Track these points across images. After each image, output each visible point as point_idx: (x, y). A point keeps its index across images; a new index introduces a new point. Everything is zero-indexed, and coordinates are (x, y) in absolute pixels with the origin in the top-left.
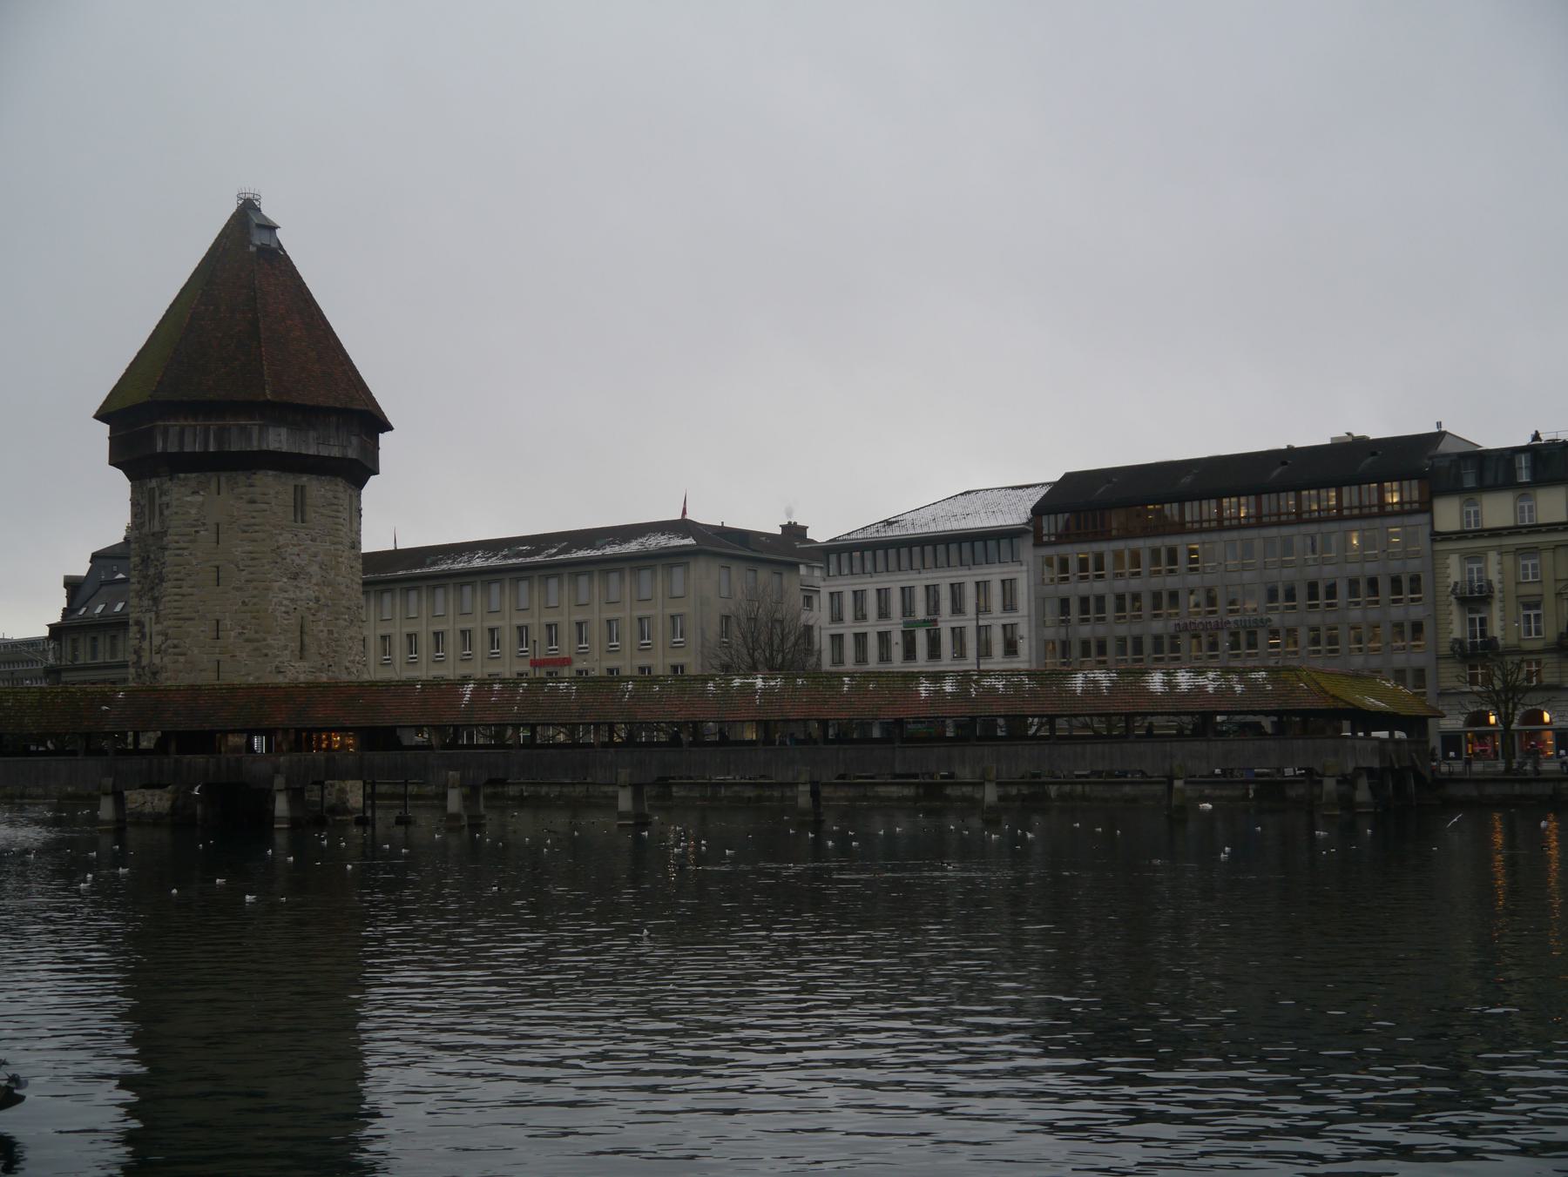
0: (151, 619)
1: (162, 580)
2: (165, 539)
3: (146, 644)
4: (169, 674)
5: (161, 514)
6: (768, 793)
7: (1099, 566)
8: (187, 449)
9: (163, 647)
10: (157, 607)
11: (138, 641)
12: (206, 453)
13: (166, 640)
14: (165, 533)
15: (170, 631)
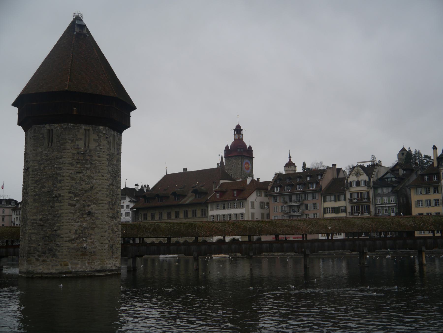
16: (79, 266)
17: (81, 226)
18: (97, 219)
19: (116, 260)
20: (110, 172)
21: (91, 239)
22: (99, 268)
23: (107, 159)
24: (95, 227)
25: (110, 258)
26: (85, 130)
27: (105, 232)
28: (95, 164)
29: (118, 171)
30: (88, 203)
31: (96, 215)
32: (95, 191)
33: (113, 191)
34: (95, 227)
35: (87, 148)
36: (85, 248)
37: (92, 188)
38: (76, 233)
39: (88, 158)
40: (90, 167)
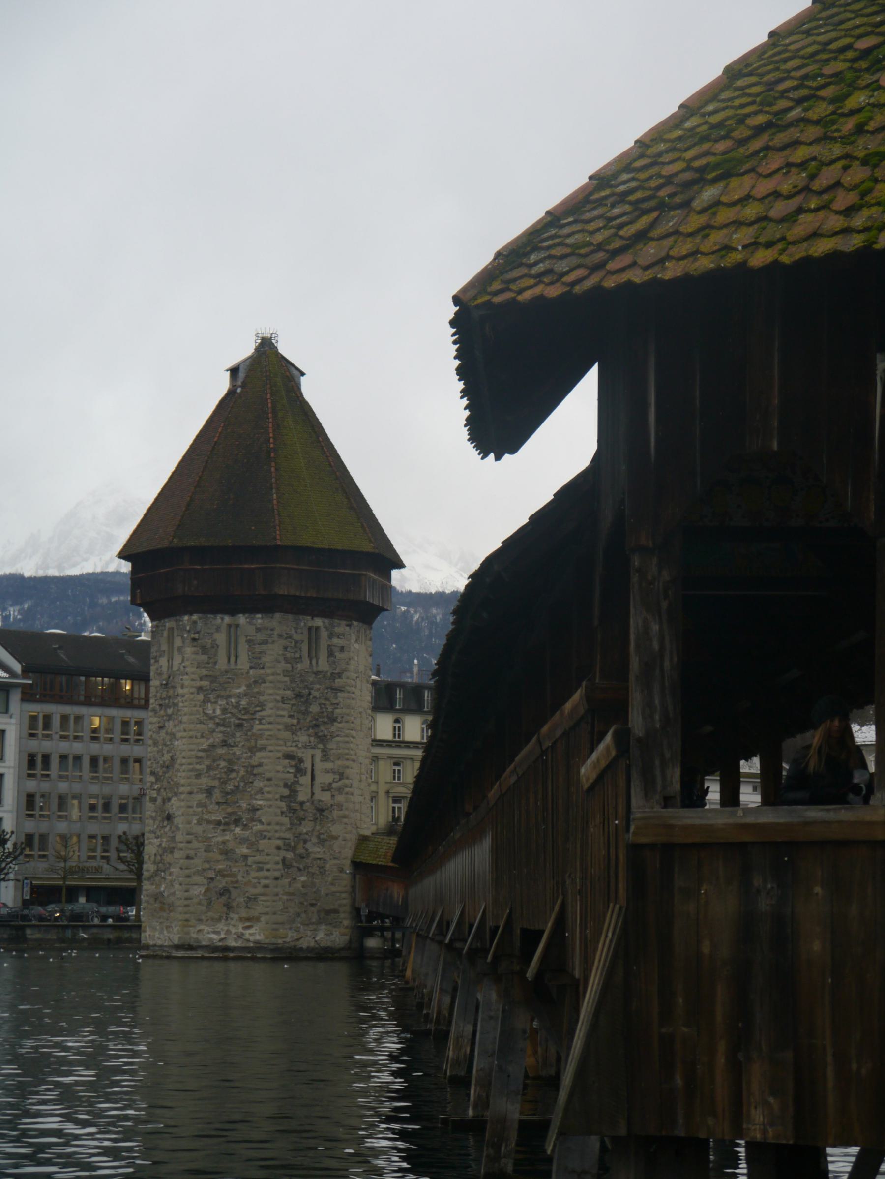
0: (313, 756)
1: (333, 720)
2: (337, 681)
3: (305, 780)
4: (347, 813)
5: (331, 654)
6: (126, 935)
7: (47, 725)
8: (375, 603)
9: (334, 785)
10: (325, 746)
11: (292, 775)
12: (379, 606)
13: (340, 780)
14: (340, 675)
15: (347, 771)
17: (160, 846)
18: (178, 828)
19: (247, 924)
20: (211, 718)
21: (171, 874)
22: (176, 942)
23: (200, 689)
24: (174, 848)
25: (219, 920)
26: (169, 628)
27: (188, 858)
29: (258, 709)
30: (170, 795)
31: (176, 821)
32: (177, 766)
33: (230, 762)
34: (174, 848)
35: (170, 670)
36: (161, 894)
37: (172, 759)
40: (173, 714)
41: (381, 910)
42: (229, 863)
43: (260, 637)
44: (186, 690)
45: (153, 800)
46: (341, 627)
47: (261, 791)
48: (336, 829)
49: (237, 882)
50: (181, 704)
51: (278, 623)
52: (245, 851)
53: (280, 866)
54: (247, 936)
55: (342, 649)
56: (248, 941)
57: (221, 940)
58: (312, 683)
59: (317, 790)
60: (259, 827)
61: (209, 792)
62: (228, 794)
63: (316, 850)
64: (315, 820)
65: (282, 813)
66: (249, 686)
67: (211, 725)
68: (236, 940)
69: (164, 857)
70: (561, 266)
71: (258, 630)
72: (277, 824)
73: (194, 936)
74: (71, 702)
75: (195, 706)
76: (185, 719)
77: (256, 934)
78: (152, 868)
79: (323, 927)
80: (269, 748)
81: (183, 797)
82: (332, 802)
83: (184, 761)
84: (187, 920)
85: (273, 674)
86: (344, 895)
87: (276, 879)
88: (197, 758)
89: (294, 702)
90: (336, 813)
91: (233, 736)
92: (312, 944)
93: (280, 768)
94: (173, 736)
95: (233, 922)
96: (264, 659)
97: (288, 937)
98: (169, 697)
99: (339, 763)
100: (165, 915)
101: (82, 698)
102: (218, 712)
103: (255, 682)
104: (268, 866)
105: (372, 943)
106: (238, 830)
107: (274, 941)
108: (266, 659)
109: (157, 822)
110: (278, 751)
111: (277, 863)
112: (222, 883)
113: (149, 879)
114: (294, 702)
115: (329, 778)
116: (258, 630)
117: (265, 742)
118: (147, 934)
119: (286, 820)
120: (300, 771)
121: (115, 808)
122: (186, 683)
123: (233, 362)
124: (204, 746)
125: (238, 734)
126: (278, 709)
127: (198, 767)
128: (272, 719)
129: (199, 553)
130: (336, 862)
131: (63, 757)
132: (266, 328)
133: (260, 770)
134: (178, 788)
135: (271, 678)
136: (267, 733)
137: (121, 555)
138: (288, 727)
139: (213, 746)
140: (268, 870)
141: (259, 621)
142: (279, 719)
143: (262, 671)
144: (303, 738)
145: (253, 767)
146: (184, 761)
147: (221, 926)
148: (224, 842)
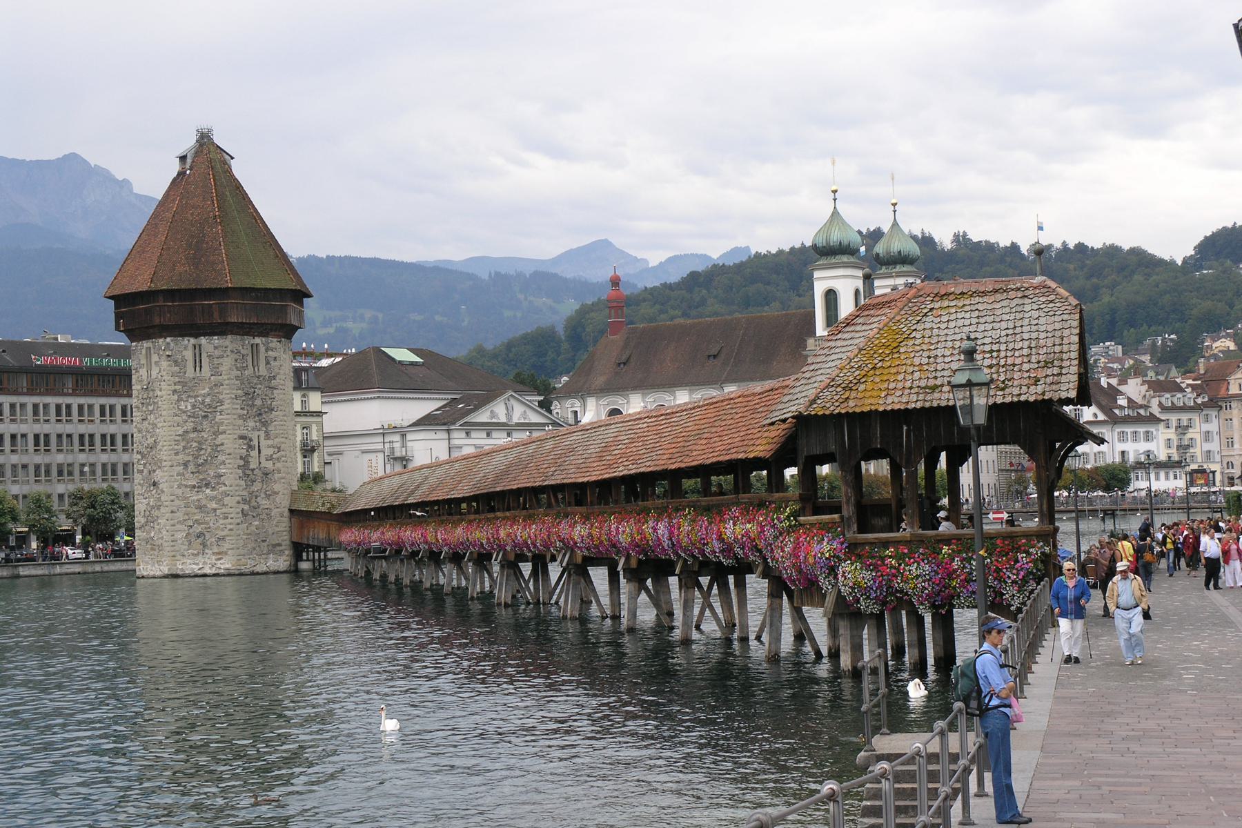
3: (254, 453)
5: (268, 363)
14: (274, 377)
15: (283, 446)
16: (149, 567)
18: (163, 492)
20: (184, 412)
21: (158, 524)
22: (166, 572)
23: (175, 391)
25: (198, 554)
26: (147, 348)
27: (172, 512)
28: (157, 403)
31: (161, 486)
32: (159, 447)
33: (199, 443)
36: (152, 538)
38: (144, 516)
39: (151, 394)
41: (311, 543)
42: (203, 515)
43: (217, 353)
44: (164, 393)
45: (142, 471)
46: (274, 342)
47: (223, 463)
48: (277, 487)
49: (209, 528)
50: (160, 403)
51: (228, 342)
52: (214, 506)
53: (240, 515)
54: (218, 566)
55: (275, 359)
56: (220, 568)
57: (199, 569)
58: (256, 384)
59: (263, 460)
60: (224, 488)
61: (186, 465)
62: (199, 465)
63: (264, 502)
64: (262, 481)
65: (240, 477)
66: (211, 388)
67: (185, 417)
68: (210, 568)
69: (152, 512)
70: (828, 405)
71: (216, 348)
72: (237, 486)
73: (180, 567)
74: (16, 393)
75: (172, 404)
76: (164, 413)
77: (226, 564)
78: (143, 521)
79: (271, 556)
80: (228, 432)
81: (166, 469)
82: (273, 468)
83: (165, 443)
84: (173, 556)
85: (228, 379)
86: (285, 533)
87: (238, 524)
88: (175, 441)
89: (244, 398)
90: (277, 476)
91: (201, 424)
92: (265, 569)
93: (237, 446)
94: (154, 425)
95: (208, 556)
96: (221, 369)
97: (248, 565)
98: (150, 398)
99: (277, 440)
100: (156, 553)
101: (25, 390)
102: (189, 408)
103: (215, 385)
104: (232, 516)
105: (305, 565)
106: (208, 491)
107: (238, 567)
108: (223, 369)
109: (145, 488)
110: (235, 434)
111: (238, 513)
112: (198, 529)
113: (140, 528)
114: (244, 398)
115: (270, 451)
116: (216, 348)
117: (224, 427)
118: (141, 567)
119: (243, 483)
120: (250, 447)
121: (54, 472)
122: (163, 387)
123: (180, 152)
124: (180, 432)
125: (205, 423)
126: (233, 403)
127: (176, 447)
128: (229, 411)
129: (171, 294)
130: (279, 510)
131: (13, 437)
132: (205, 124)
133: (222, 448)
134: (161, 463)
135: (226, 382)
136: (226, 421)
137: (107, 295)
138: (240, 417)
139: (186, 432)
140: (232, 518)
141: (216, 341)
142: (234, 412)
143: (220, 377)
144: (251, 424)
145: (217, 446)
146: (165, 443)
147: (200, 559)
148: (198, 500)
